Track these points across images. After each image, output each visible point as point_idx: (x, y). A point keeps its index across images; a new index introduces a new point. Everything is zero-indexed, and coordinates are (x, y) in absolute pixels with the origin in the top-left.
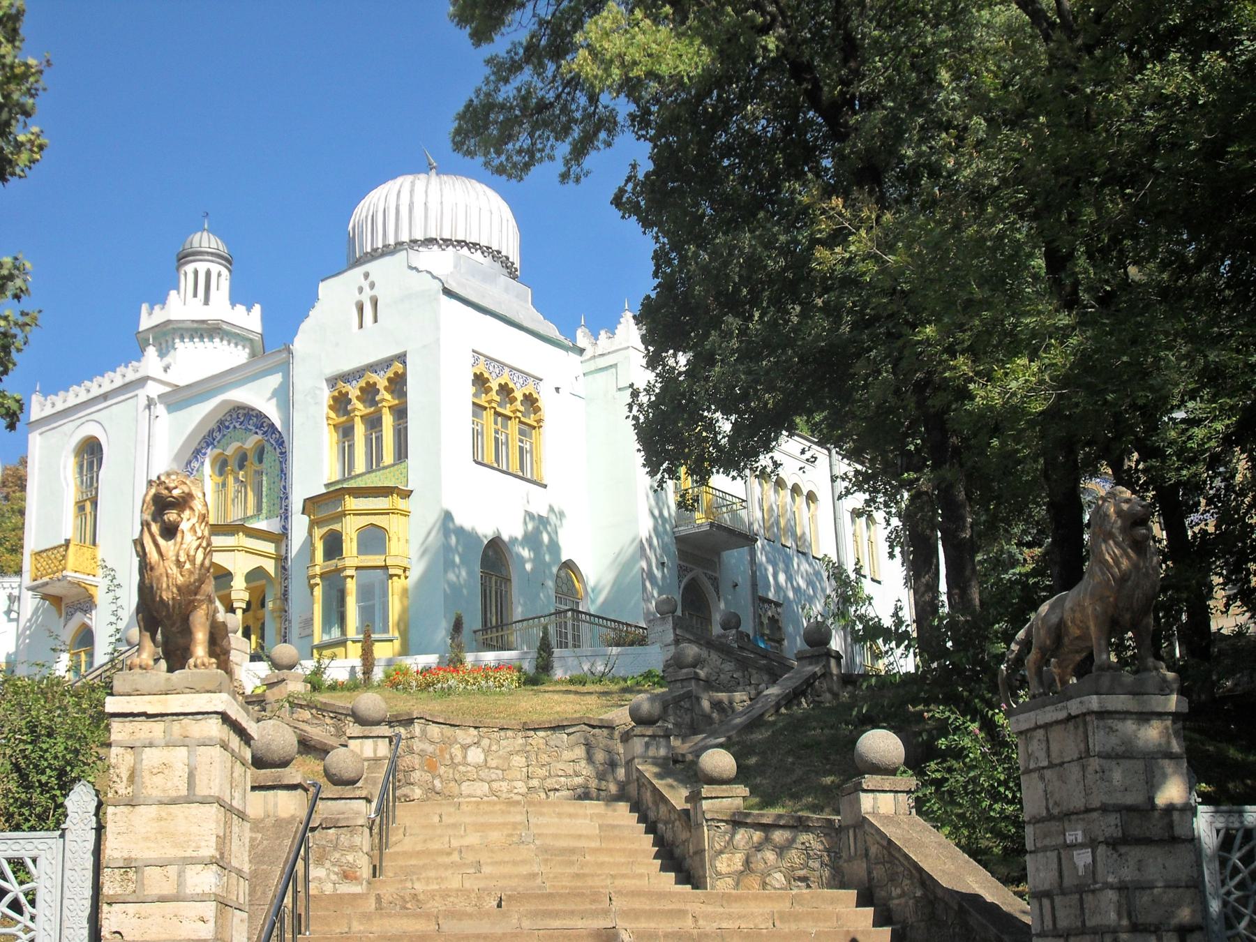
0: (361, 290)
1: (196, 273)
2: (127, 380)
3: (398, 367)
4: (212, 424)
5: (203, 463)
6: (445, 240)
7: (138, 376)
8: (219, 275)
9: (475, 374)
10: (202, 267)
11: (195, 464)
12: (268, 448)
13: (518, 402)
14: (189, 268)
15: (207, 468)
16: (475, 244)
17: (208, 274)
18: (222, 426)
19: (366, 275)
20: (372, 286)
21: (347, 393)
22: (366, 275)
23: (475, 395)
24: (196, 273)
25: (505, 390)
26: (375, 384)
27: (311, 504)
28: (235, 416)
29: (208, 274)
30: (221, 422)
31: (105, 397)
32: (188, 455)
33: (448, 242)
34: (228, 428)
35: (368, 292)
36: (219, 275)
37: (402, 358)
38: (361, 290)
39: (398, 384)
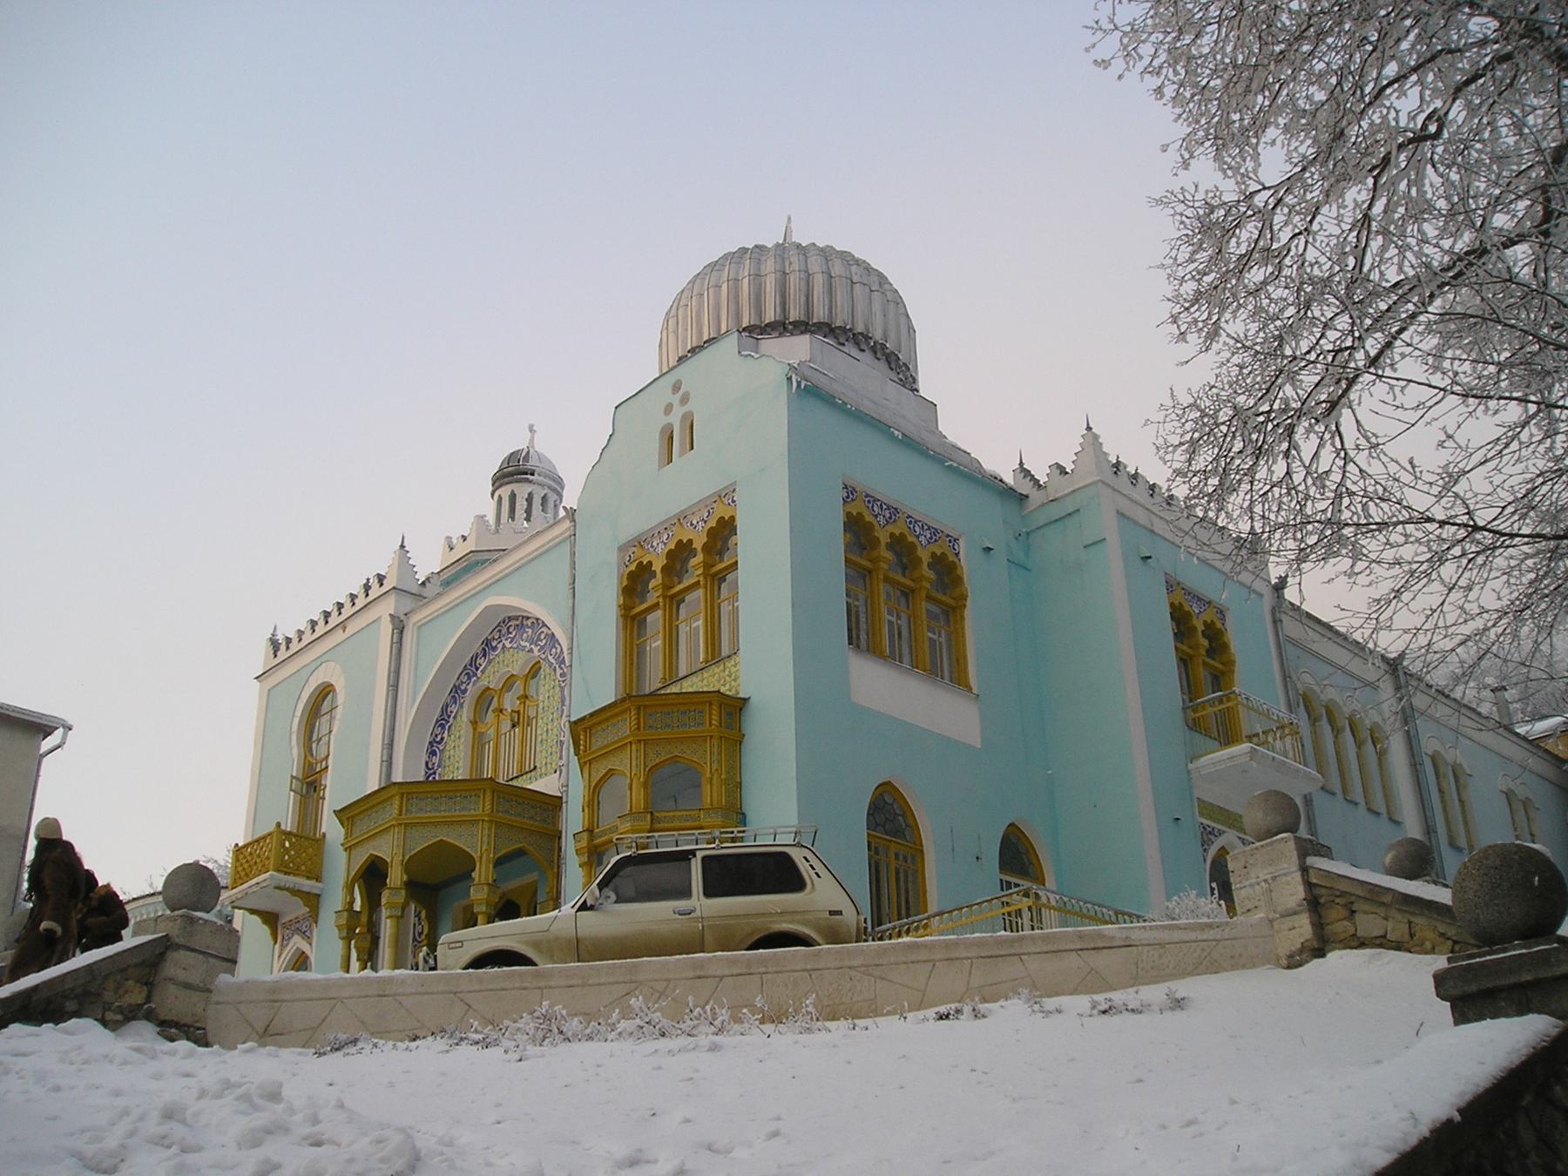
0: (668, 409)
1: (513, 497)
2: (370, 598)
3: (722, 511)
4: (476, 648)
5: (461, 705)
6: (796, 324)
7: (384, 589)
8: (544, 499)
9: (848, 515)
10: (522, 491)
11: (454, 708)
12: (544, 665)
13: (925, 566)
14: (505, 492)
15: (465, 715)
16: (843, 329)
17: (530, 499)
18: (487, 646)
19: (677, 387)
20: (685, 400)
21: (650, 563)
22: (677, 387)
23: (847, 546)
24: (513, 497)
25: (900, 546)
26: (690, 541)
27: (582, 729)
28: (504, 631)
29: (530, 499)
30: (487, 642)
31: (342, 625)
32: (444, 697)
33: (803, 327)
34: (495, 649)
35: (678, 412)
36: (544, 499)
37: (726, 495)
38: (668, 409)
39: (723, 532)
